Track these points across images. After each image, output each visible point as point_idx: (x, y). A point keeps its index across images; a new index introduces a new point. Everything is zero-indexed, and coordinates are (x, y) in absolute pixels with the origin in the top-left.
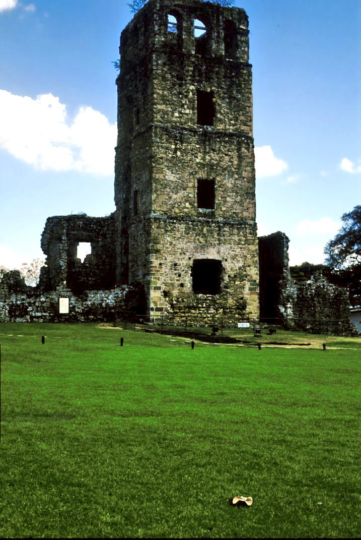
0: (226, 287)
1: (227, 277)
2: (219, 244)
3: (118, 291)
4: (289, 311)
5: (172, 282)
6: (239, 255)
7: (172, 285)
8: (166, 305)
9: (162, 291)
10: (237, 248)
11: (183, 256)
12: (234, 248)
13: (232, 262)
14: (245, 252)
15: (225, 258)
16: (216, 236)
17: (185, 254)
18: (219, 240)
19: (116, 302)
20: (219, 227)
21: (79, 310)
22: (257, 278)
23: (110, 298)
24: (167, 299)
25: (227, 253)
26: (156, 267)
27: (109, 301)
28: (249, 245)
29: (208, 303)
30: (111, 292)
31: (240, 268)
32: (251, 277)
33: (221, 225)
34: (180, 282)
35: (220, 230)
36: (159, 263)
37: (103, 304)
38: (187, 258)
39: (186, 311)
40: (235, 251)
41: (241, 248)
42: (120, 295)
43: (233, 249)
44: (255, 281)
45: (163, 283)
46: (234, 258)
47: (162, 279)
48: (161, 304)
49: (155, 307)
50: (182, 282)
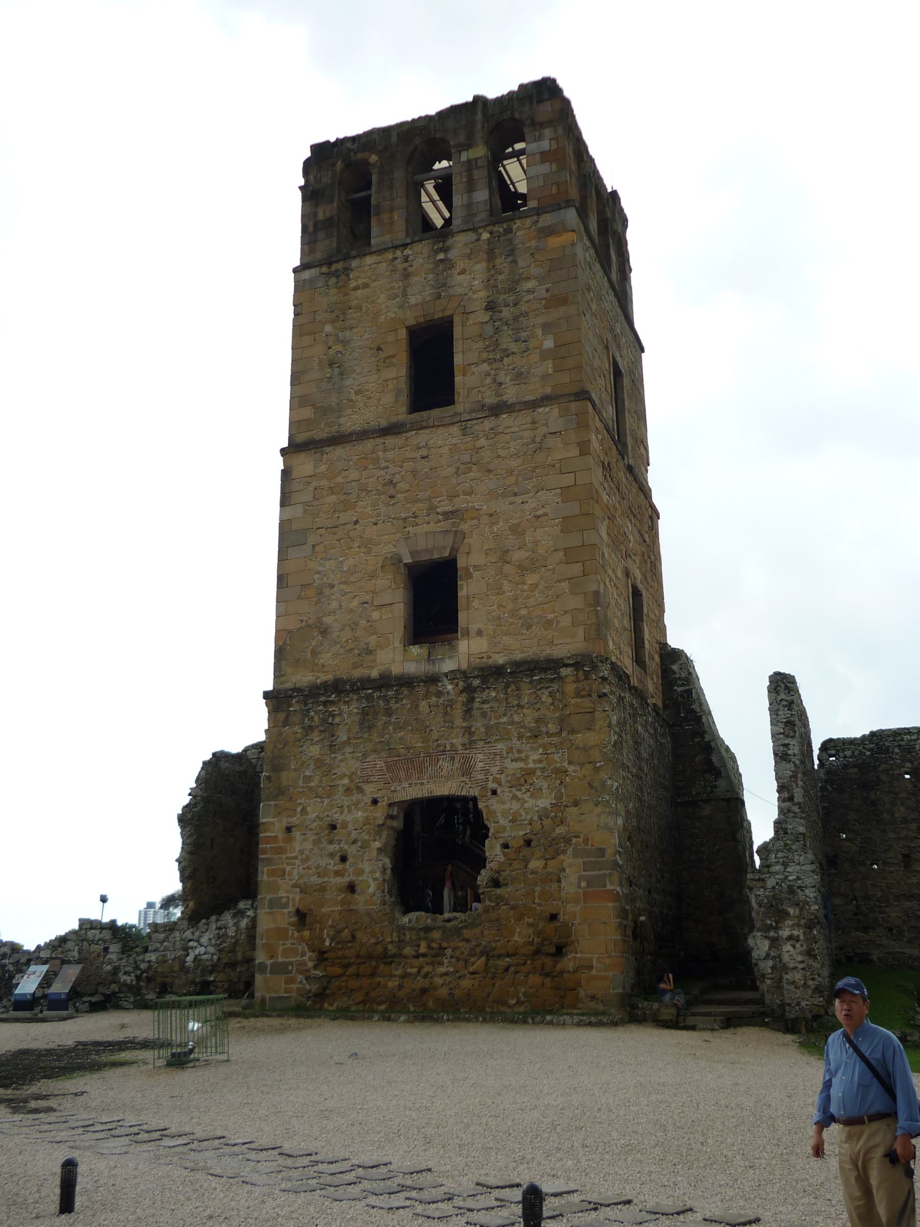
0: (496, 883)
1: (498, 849)
2: (470, 745)
3: (227, 918)
4: (790, 953)
5: (320, 880)
6: (538, 773)
7: (322, 889)
8: (303, 955)
9: (291, 909)
10: (532, 749)
11: (354, 798)
12: (519, 751)
13: (515, 797)
14: (559, 759)
15: (492, 785)
16: (459, 722)
17: (360, 790)
18: (468, 731)
19: (220, 951)
20: (469, 690)
21: (128, 979)
22: (612, 842)
23: (205, 940)
24: (306, 933)
25: (495, 770)
26: (276, 837)
27: (202, 950)
28: (573, 732)
29: (433, 941)
30: (207, 924)
31: (543, 815)
32: (586, 841)
33: (476, 682)
34: (345, 880)
35: (471, 700)
36: (285, 825)
37: (188, 959)
38: (368, 800)
39: (362, 969)
40: (525, 760)
41: (544, 746)
42: (231, 932)
43: (516, 755)
44: (602, 852)
45: (295, 886)
46: (523, 780)
47: (296, 872)
48: (286, 953)
49: (269, 962)
50: (352, 878)
